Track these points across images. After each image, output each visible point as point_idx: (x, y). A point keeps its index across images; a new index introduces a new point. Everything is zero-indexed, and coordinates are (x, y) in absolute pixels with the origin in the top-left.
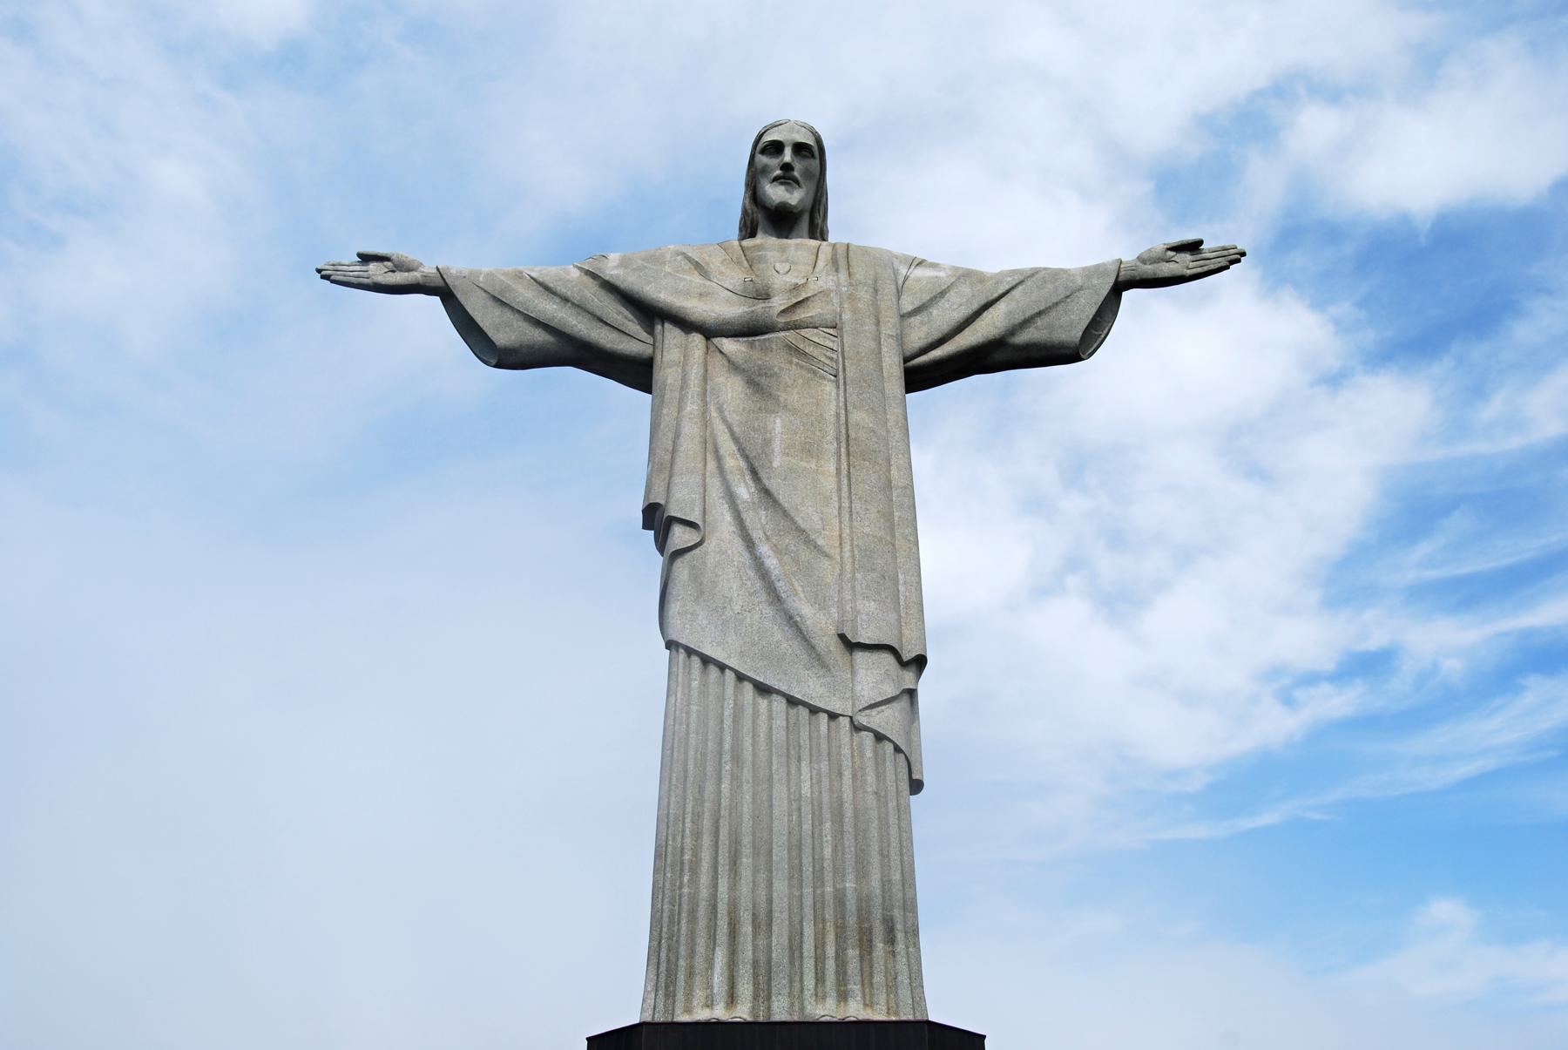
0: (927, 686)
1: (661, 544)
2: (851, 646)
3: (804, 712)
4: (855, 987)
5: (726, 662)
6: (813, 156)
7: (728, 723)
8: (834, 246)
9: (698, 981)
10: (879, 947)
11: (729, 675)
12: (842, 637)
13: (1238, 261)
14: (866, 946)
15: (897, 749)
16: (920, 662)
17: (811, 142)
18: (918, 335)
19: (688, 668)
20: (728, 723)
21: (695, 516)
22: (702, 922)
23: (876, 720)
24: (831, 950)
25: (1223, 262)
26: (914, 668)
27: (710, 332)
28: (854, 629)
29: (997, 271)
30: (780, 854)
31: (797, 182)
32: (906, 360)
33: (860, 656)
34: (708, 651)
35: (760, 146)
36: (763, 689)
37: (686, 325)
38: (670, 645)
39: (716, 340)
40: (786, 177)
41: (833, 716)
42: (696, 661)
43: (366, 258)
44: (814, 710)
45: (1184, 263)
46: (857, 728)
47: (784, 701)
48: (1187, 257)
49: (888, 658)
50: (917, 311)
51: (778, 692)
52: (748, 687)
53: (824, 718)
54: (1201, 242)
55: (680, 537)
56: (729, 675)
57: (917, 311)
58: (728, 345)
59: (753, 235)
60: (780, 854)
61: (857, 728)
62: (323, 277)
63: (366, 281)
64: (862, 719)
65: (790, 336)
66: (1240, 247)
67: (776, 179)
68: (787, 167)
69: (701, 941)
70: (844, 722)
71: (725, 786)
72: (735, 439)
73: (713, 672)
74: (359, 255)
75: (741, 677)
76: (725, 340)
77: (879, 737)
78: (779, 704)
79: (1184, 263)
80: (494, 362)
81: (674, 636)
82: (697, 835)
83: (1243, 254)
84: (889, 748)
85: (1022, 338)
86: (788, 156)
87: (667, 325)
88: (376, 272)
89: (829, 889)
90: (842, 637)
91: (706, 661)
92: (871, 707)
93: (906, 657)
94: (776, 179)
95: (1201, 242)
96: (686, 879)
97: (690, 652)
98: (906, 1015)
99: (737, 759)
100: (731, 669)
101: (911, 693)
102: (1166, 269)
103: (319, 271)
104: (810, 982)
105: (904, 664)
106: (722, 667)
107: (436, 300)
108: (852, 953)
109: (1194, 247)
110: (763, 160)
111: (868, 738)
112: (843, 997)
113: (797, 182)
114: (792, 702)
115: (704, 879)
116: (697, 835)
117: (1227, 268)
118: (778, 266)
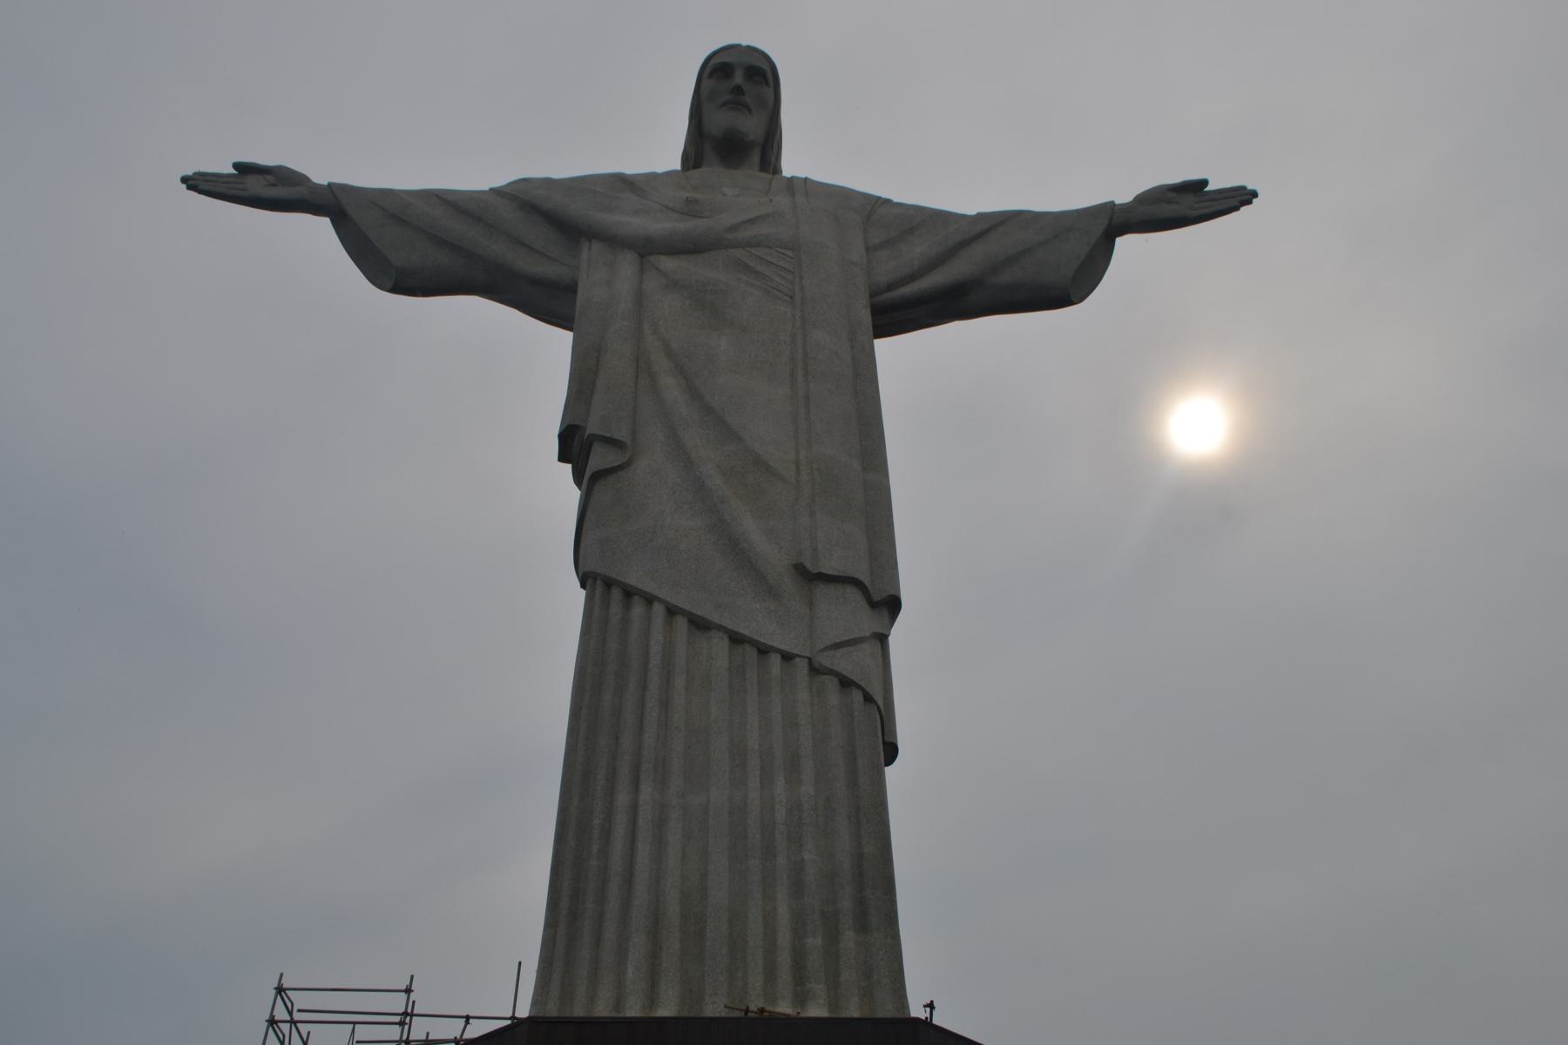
0: (900, 636)
1: (578, 478)
2: (809, 578)
3: (751, 653)
4: (819, 988)
5: (656, 592)
6: (767, 83)
7: (655, 662)
8: (792, 180)
10: (849, 939)
11: (658, 609)
12: (800, 570)
13: (1249, 202)
14: (833, 937)
15: (868, 699)
16: (892, 606)
17: (766, 68)
18: (888, 267)
19: (606, 604)
20: (655, 662)
21: (622, 434)
22: (613, 904)
23: (843, 663)
24: (784, 938)
25: (1234, 203)
26: (885, 613)
27: (646, 249)
29: (971, 211)
31: (749, 110)
32: (873, 295)
33: (822, 590)
34: (633, 580)
35: (708, 70)
36: (699, 625)
37: (616, 242)
38: (583, 586)
39: (652, 258)
40: (737, 100)
41: (787, 657)
42: (616, 595)
44: (763, 651)
45: (1187, 204)
46: (815, 670)
47: (726, 640)
49: (852, 593)
50: (887, 244)
51: (720, 628)
52: (681, 623)
53: (776, 659)
54: (1204, 183)
55: (599, 458)
56: (658, 609)
57: (887, 244)
58: (668, 263)
59: (697, 166)
61: (815, 670)
62: (189, 188)
63: (241, 193)
64: (825, 660)
65: (739, 253)
66: (1250, 187)
67: (724, 105)
68: (738, 90)
70: (802, 667)
73: (638, 609)
74: (236, 166)
75: (672, 611)
76: (663, 258)
77: (846, 683)
78: (720, 644)
79: (1187, 204)
80: (390, 285)
81: (592, 566)
83: (1254, 194)
84: (857, 697)
85: (1005, 278)
86: (738, 78)
87: (597, 246)
88: (255, 185)
89: (781, 860)
90: (800, 570)
91: (629, 593)
92: (837, 646)
93: (876, 597)
94: (724, 105)
95: (1204, 183)
96: (595, 848)
97: (609, 583)
98: (886, 1010)
99: (665, 704)
100: (659, 600)
101: (882, 639)
102: (1167, 210)
103: (184, 180)
105: (873, 605)
106: (650, 600)
107: (325, 222)
108: (815, 942)
110: (707, 84)
111: (831, 684)
112: (801, 998)
113: (749, 110)
114: (736, 639)
117: (1236, 209)
118: (725, 189)
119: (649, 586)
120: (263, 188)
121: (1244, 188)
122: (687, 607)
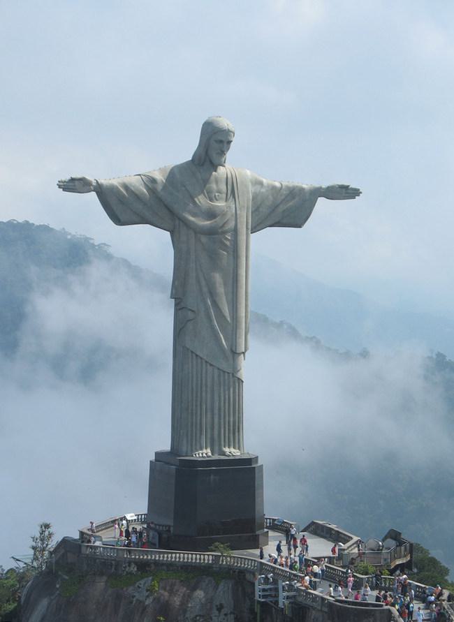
9: (198, 444)
11: (204, 362)
20: (204, 375)
24: (227, 435)
28: (236, 349)
30: (216, 411)
34: (198, 354)
36: (211, 365)
43: (72, 180)
44: (224, 372)
48: (344, 190)
52: (208, 365)
53: (226, 374)
58: (204, 239)
60: (216, 411)
69: (198, 432)
70: (231, 375)
71: (204, 394)
72: (205, 279)
75: (206, 362)
82: (196, 406)
99: (206, 386)
104: (223, 443)
108: (232, 435)
109: (346, 187)
114: (218, 369)
115: (199, 418)
116: (196, 406)
119: (201, 355)
120: (74, 185)
121: (359, 190)
122: (210, 362)
